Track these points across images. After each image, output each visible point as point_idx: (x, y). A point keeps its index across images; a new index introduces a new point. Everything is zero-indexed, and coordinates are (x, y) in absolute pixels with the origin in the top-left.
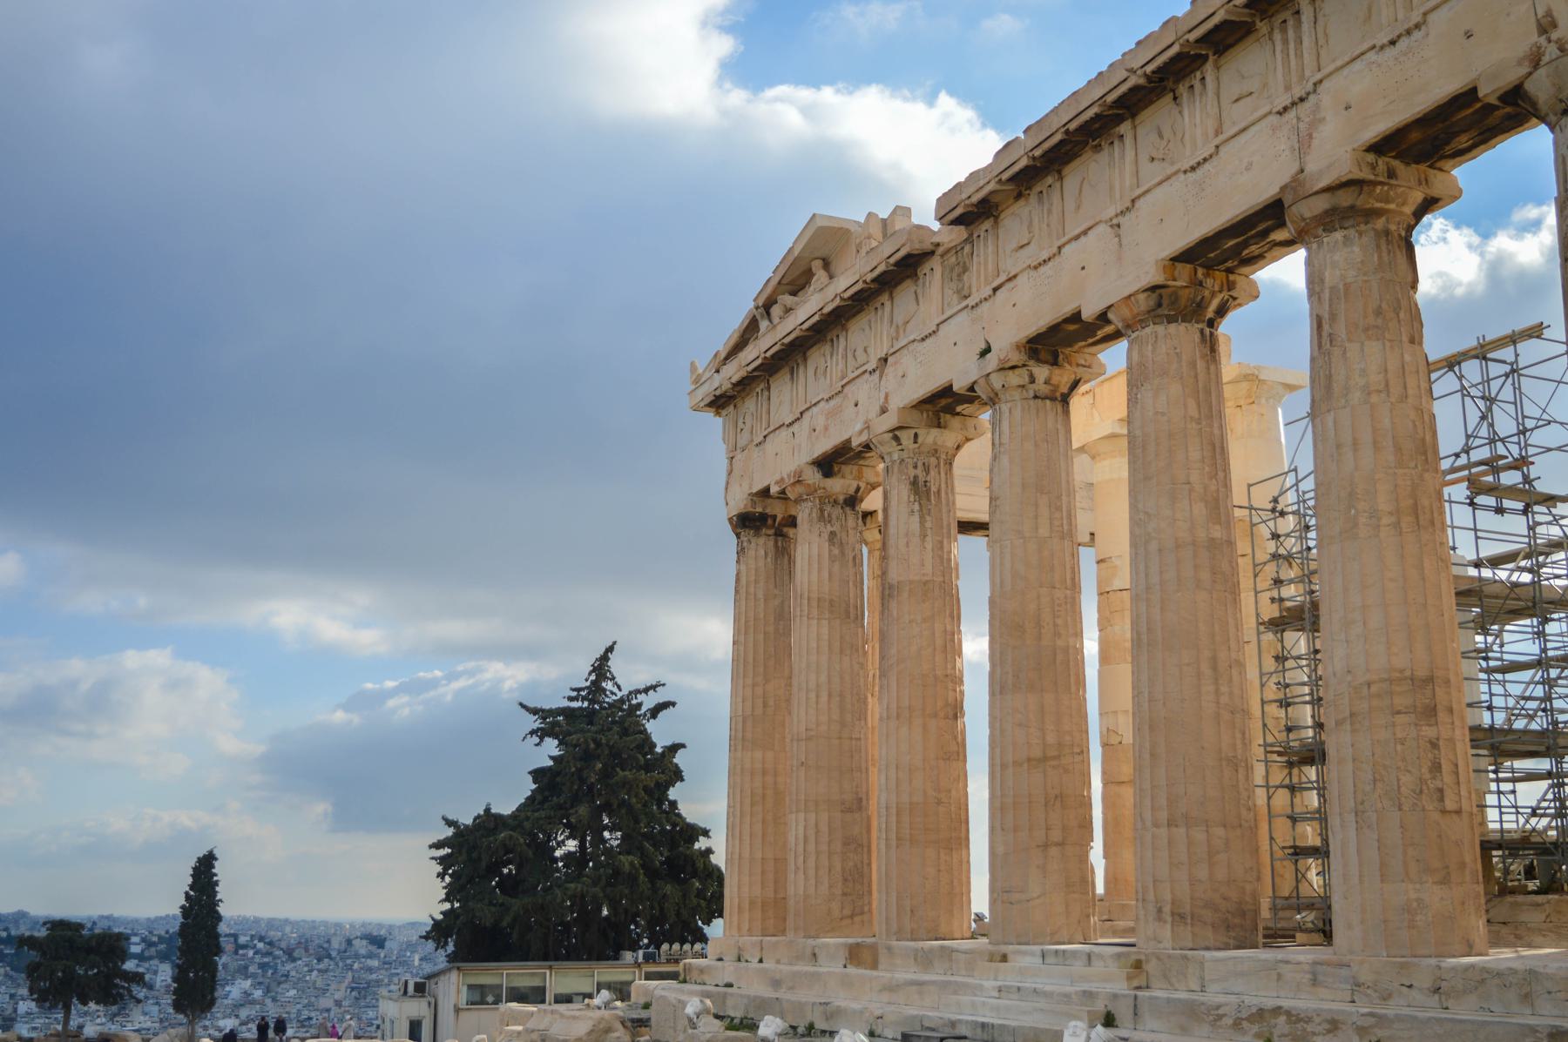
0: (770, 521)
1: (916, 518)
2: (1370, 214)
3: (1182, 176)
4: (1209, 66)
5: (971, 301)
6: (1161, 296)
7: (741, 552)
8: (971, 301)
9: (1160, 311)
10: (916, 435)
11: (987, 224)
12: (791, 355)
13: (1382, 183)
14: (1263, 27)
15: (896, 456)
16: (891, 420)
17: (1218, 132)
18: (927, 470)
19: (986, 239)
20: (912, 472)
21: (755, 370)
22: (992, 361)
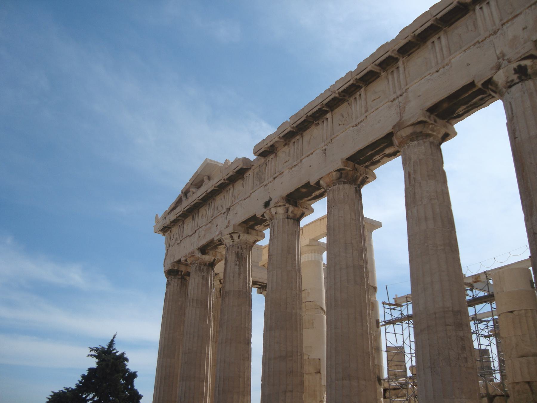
0: (180, 273)
1: (237, 267)
2: (428, 135)
3: (351, 128)
4: (362, 90)
5: (265, 183)
6: (341, 174)
7: (168, 284)
8: (265, 183)
9: (341, 180)
10: (239, 236)
11: (273, 156)
12: (193, 211)
13: (432, 124)
14: (383, 74)
15: (231, 244)
16: (230, 230)
17: (366, 111)
18: (242, 249)
19: (272, 161)
20: (237, 250)
21: (179, 216)
22: (272, 204)
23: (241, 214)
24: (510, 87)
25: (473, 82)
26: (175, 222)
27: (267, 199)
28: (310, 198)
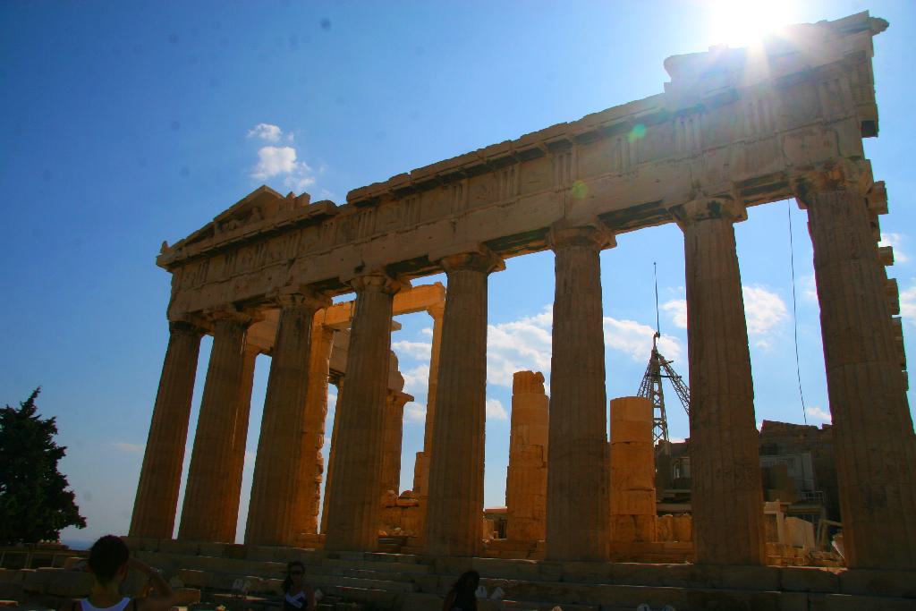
0: (192, 328)
3: (495, 207)
4: (517, 165)
10: (304, 299)
11: (372, 209)
16: (294, 289)
17: (519, 194)
18: (305, 316)
21: (206, 252)
22: (366, 271)
23: (313, 271)
24: (699, 220)
25: (661, 201)
26: (193, 259)
27: (360, 264)
28: (413, 272)
